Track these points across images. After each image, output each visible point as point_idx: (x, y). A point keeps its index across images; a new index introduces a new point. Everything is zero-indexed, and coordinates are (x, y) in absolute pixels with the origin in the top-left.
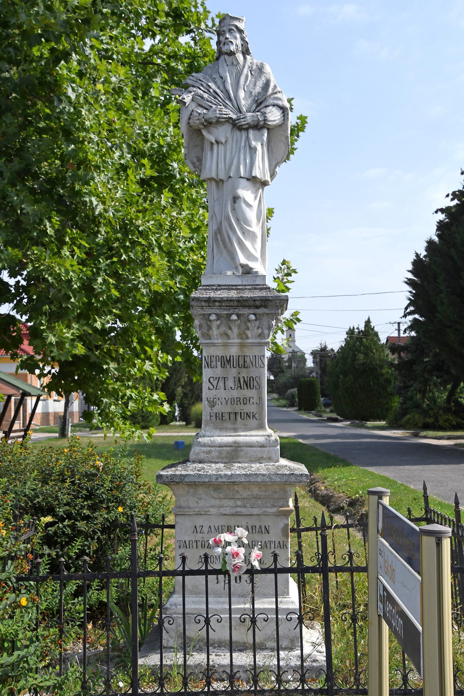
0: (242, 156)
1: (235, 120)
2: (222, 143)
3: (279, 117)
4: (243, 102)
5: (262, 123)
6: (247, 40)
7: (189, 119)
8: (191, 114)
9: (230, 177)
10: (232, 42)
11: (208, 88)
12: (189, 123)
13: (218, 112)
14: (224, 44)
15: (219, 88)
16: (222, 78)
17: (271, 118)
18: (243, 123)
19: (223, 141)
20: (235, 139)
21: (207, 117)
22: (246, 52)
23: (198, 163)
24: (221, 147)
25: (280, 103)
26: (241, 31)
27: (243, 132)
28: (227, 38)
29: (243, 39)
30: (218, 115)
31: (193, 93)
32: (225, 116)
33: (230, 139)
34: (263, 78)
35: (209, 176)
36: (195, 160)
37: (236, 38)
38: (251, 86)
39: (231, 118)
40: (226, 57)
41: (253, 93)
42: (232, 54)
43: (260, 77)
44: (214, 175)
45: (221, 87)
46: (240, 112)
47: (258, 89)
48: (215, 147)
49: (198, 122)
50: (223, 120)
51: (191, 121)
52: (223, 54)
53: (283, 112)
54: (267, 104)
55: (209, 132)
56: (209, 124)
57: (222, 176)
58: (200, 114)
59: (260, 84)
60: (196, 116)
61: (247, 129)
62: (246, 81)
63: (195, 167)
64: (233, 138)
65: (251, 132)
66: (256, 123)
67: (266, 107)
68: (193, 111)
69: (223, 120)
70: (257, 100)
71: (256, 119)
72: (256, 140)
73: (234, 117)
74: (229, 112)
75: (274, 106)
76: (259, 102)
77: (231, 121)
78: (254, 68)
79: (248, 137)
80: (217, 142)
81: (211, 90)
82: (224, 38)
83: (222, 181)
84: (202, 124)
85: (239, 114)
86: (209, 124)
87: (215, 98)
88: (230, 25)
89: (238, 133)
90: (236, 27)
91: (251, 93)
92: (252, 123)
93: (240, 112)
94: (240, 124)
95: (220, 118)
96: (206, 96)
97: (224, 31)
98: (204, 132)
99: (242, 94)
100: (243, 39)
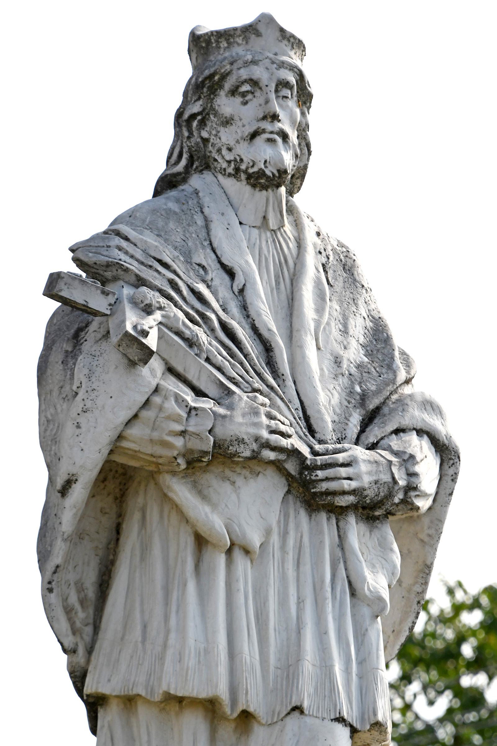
2: (247, 552)
8: (147, 403)
9: (298, 709)
14: (254, 135)
16: (231, 273)
19: (255, 539)
20: (291, 542)
21: (226, 431)
30: (265, 434)
36: (73, 599)
44: (222, 691)
49: (179, 442)
51: (135, 431)
54: (406, 422)
58: (191, 410)
60: (177, 419)
62: (320, 310)
64: (284, 536)
68: (157, 390)
71: (385, 478)
75: (420, 432)
88: (282, 65)
91: (337, 361)
93: (312, 431)
94: (333, 486)
95: (267, 445)
97: (255, 83)
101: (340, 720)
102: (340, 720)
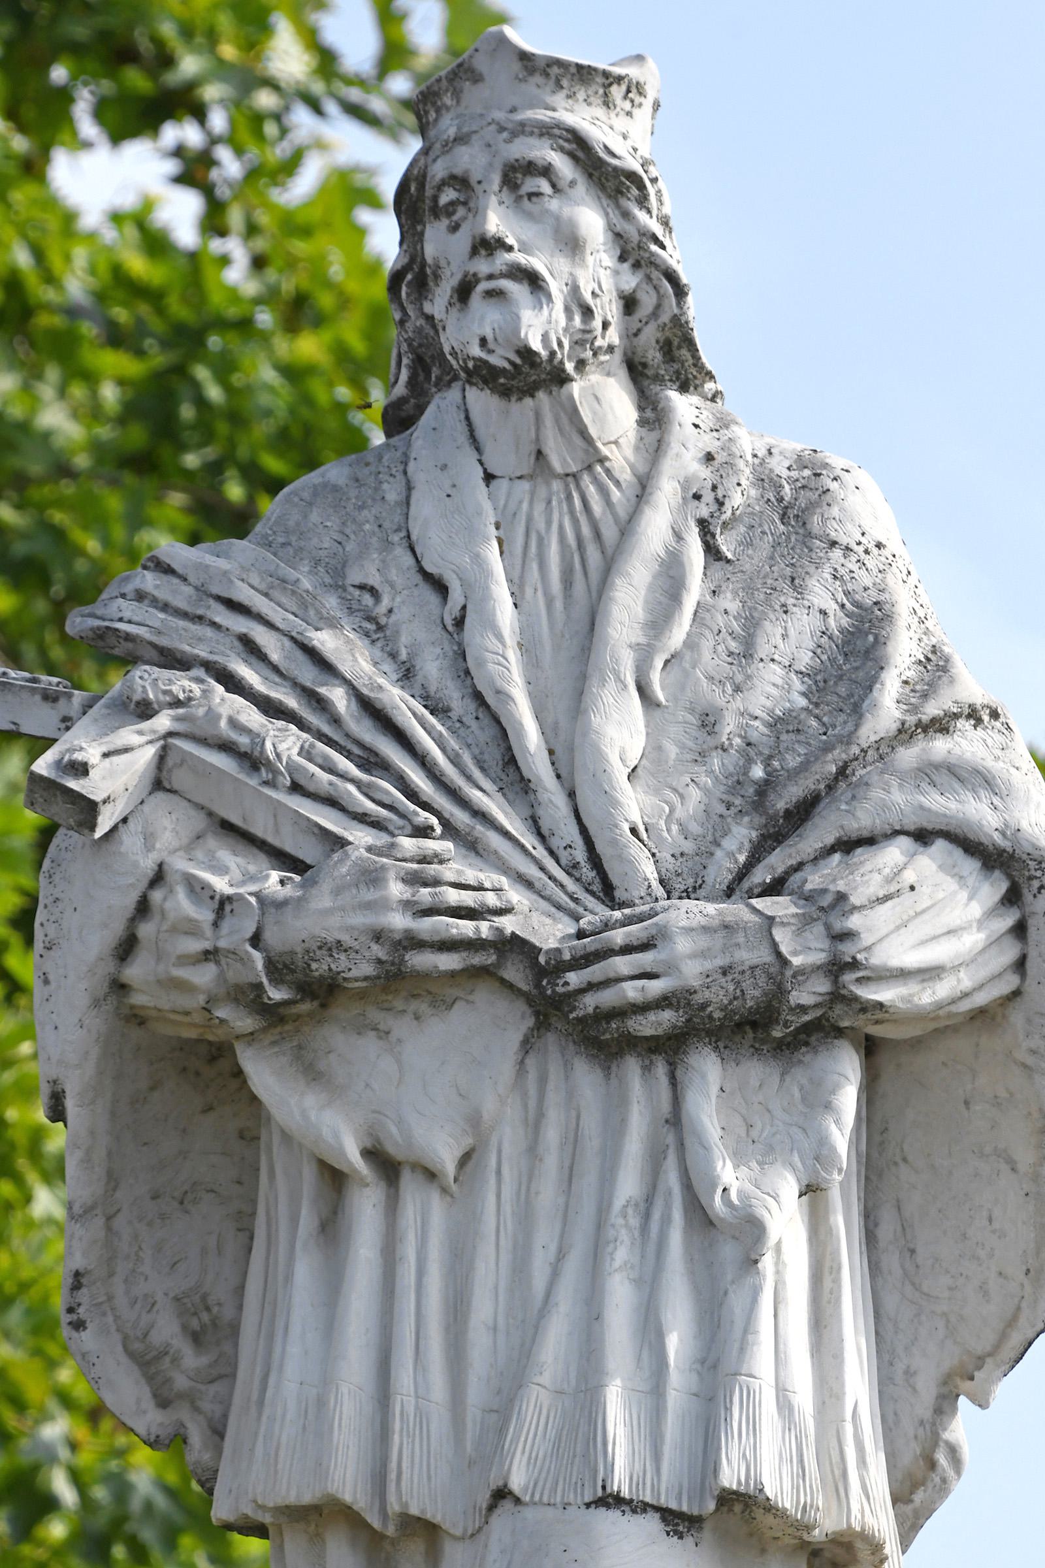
0: (620, 1297)
1: (559, 967)
3: (974, 939)
4: (633, 804)
5: (808, 994)
6: (674, 256)
7: (127, 947)
8: (143, 908)
9: (501, 1494)
10: (533, 280)
11: (307, 674)
12: (120, 987)
13: (396, 889)
14: (464, 292)
15: (407, 675)
16: (440, 587)
17: (899, 952)
18: (632, 991)
20: (552, 1135)
21: (287, 934)
22: (664, 359)
23: (191, 1360)
25: (980, 814)
26: (616, 184)
27: (632, 1066)
28: (488, 246)
29: (635, 251)
30: (399, 921)
31: (163, 722)
32: (465, 928)
33: (508, 1138)
34: (822, 593)
35: (297, 1490)
36: (167, 1330)
37: (571, 243)
38: (712, 657)
39: (514, 945)
40: (480, 400)
41: (729, 726)
42: (531, 376)
44: (347, 1481)
45: (433, 668)
46: (607, 892)
47: (774, 688)
48: (366, 1206)
49: (204, 976)
50: (448, 962)
52: (449, 378)
53: (1012, 897)
54: (863, 820)
55: (312, 1073)
56: (308, 995)
57: (425, 1482)
58: (223, 905)
59: (795, 638)
60: (191, 929)
61: (670, 1048)
63: (163, 1403)
64: (535, 1125)
65: (708, 1075)
66: (754, 993)
67: (847, 845)
68: (159, 877)
69: (448, 962)
70: (764, 789)
71: (754, 955)
72: (755, 1148)
73: (549, 932)
75: (923, 837)
76: (782, 802)
77: (515, 973)
78: (736, 500)
79: (676, 1119)
80: (387, 1165)
81: (338, 696)
82: (462, 242)
83: (426, 1531)
84: (249, 996)
85: (596, 913)
86: (308, 995)
87: (372, 762)
88: (522, 129)
89: (586, 1077)
90: (579, 147)
91: (708, 722)
92: (717, 996)
94: (606, 998)
95: (414, 942)
96: (285, 744)
97: (461, 182)
98: (264, 1073)
99: (621, 731)
100: (635, 251)
101: (610, 1501)
102: (610, 1501)
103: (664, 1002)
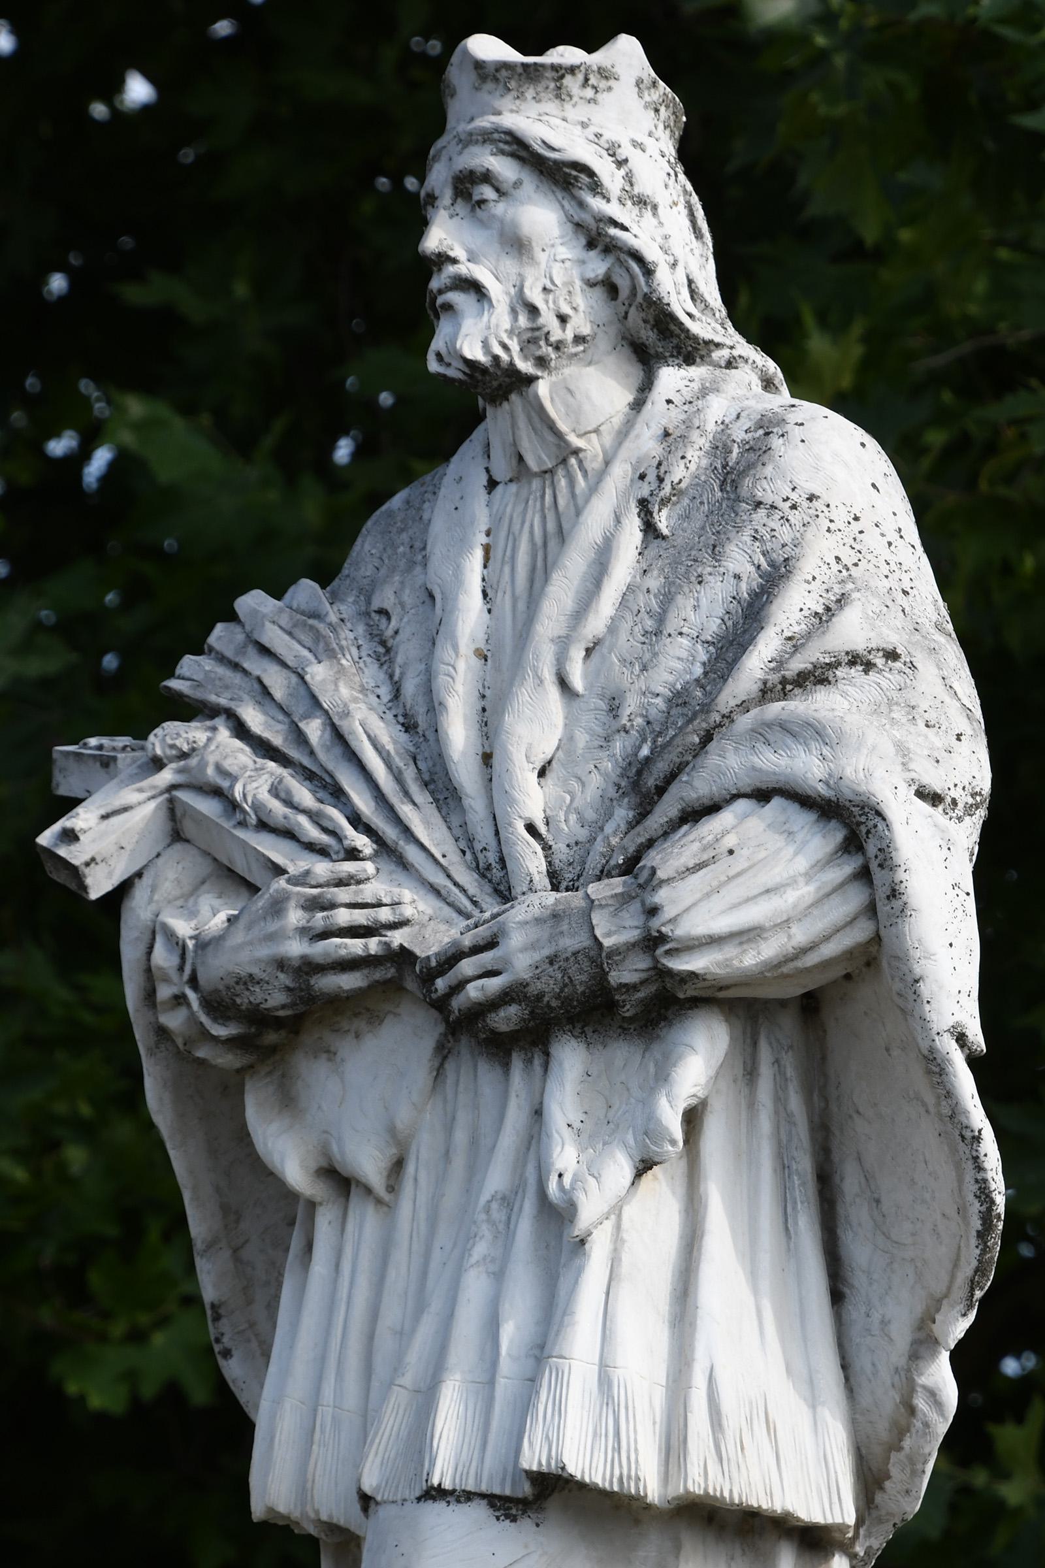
2: (368, 1191)
3: (804, 892)
4: (532, 799)
10: (474, 287)
13: (295, 917)
18: (473, 991)
20: (461, 1137)
24: (365, 1222)
25: (808, 767)
26: (563, 177)
29: (597, 237)
30: (296, 948)
31: (166, 776)
32: (355, 946)
37: (517, 245)
41: (631, 704)
43: (716, 551)
47: (680, 660)
50: (349, 981)
66: (581, 978)
69: (349, 981)
71: (573, 942)
72: (596, 1133)
74: (414, 903)
75: (762, 795)
78: (678, 473)
81: (314, 729)
89: (487, 1074)
90: (518, 147)
92: (548, 985)
95: (309, 968)
99: (539, 725)
100: (597, 237)
101: (435, 1494)
103: (506, 997)
